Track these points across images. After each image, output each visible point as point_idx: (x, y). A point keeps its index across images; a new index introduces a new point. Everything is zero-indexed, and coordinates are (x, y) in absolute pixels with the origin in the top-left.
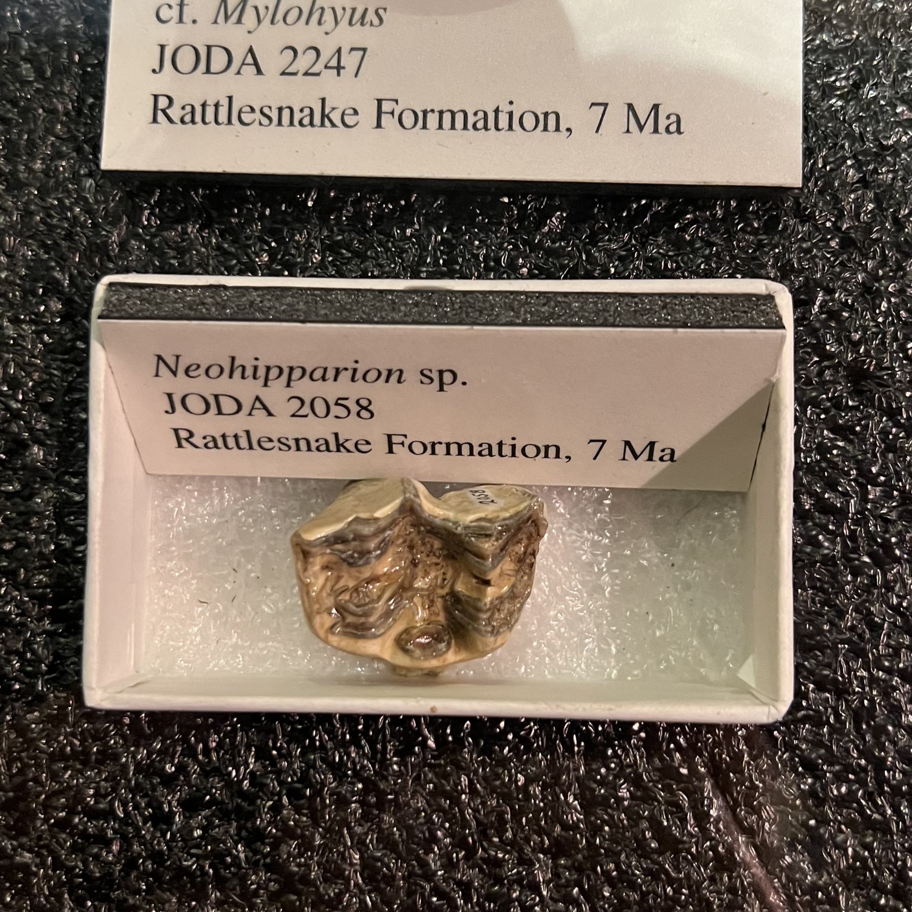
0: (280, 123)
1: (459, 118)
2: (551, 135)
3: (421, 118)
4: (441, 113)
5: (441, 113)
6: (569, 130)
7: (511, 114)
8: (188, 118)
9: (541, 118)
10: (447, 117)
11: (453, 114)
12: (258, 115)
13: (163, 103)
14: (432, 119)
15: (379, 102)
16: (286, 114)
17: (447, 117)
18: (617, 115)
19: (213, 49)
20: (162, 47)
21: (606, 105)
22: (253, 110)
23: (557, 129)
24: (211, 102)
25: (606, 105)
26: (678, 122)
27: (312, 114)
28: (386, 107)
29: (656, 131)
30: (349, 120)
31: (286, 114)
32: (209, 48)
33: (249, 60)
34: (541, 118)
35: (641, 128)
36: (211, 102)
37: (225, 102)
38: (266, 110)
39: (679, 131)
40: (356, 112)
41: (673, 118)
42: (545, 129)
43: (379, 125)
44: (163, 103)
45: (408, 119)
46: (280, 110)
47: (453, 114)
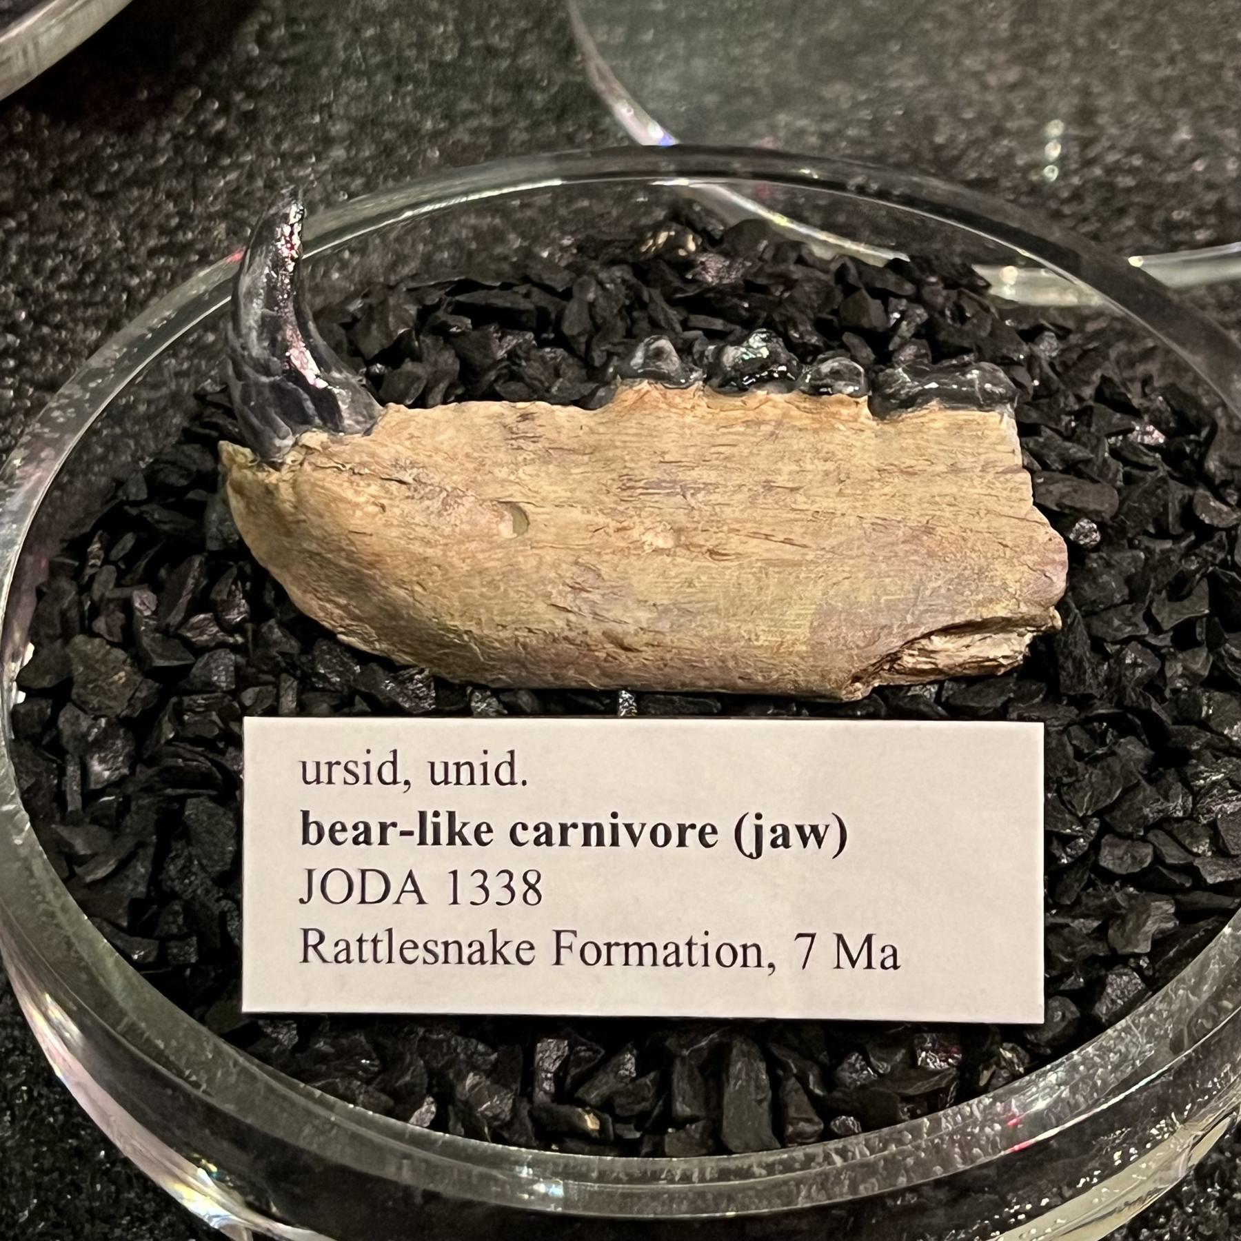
0: (446, 961)
1: (648, 951)
2: (752, 969)
3: (604, 952)
4: (627, 946)
5: (627, 946)
6: (771, 965)
7: (706, 946)
8: (342, 957)
9: (740, 951)
10: (634, 951)
11: (641, 947)
12: (421, 952)
13: (313, 938)
14: (618, 954)
15: (558, 933)
16: (453, 949)
17: (634, 951)
18: (826, 946)
19: (368, 874)
20: (310, 872)
21: (813, 936)
22: (416, 947)
23: (759, 965)
24: (368, 937)
25: (813, 936)
26: (895, 955)
27: (482, 950)
28: (566, 939)
29: (869, 966)
30: (525, 956)
31: (453, 949)
32: (363, 872)
33: (410, 887)
34: (740, 951)
35: (853, 963)
36: (368, 937)
37: (384, 937)
38: (430, 946)
39: (895, 967)
40: (532, 948)
41: (889, 951)
42: (745, 965)
43: (558, 962)
44: (313, 938)
45: (591, 954)
46: (446, 944)
47: (641, 947)
